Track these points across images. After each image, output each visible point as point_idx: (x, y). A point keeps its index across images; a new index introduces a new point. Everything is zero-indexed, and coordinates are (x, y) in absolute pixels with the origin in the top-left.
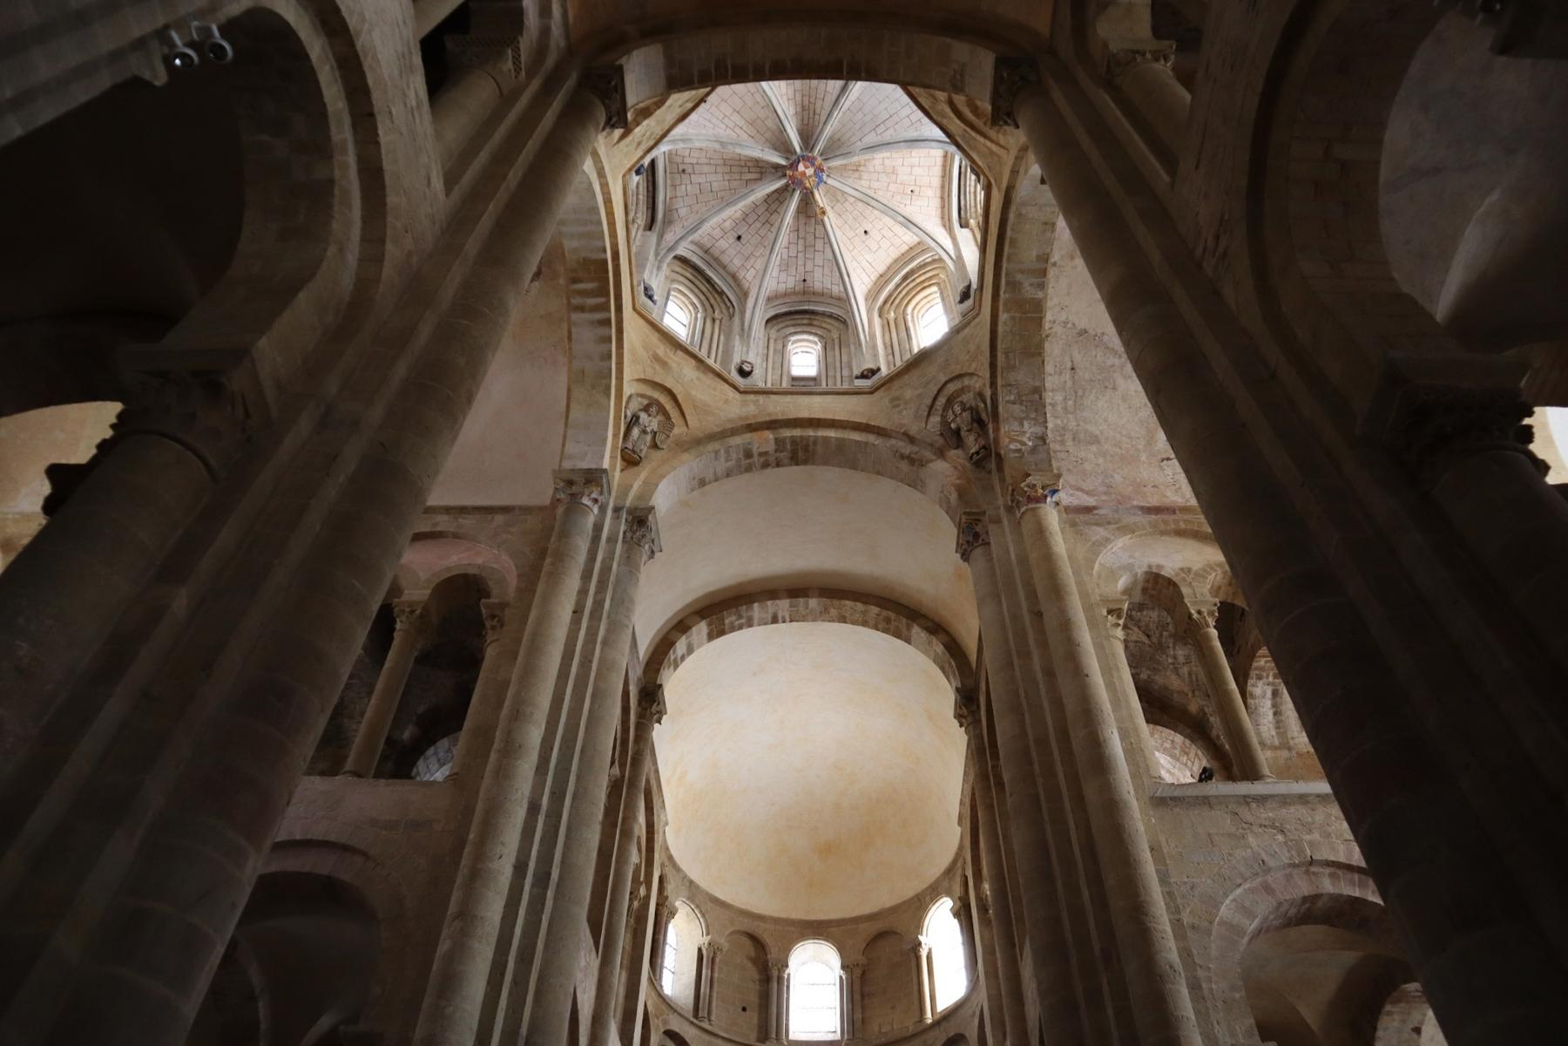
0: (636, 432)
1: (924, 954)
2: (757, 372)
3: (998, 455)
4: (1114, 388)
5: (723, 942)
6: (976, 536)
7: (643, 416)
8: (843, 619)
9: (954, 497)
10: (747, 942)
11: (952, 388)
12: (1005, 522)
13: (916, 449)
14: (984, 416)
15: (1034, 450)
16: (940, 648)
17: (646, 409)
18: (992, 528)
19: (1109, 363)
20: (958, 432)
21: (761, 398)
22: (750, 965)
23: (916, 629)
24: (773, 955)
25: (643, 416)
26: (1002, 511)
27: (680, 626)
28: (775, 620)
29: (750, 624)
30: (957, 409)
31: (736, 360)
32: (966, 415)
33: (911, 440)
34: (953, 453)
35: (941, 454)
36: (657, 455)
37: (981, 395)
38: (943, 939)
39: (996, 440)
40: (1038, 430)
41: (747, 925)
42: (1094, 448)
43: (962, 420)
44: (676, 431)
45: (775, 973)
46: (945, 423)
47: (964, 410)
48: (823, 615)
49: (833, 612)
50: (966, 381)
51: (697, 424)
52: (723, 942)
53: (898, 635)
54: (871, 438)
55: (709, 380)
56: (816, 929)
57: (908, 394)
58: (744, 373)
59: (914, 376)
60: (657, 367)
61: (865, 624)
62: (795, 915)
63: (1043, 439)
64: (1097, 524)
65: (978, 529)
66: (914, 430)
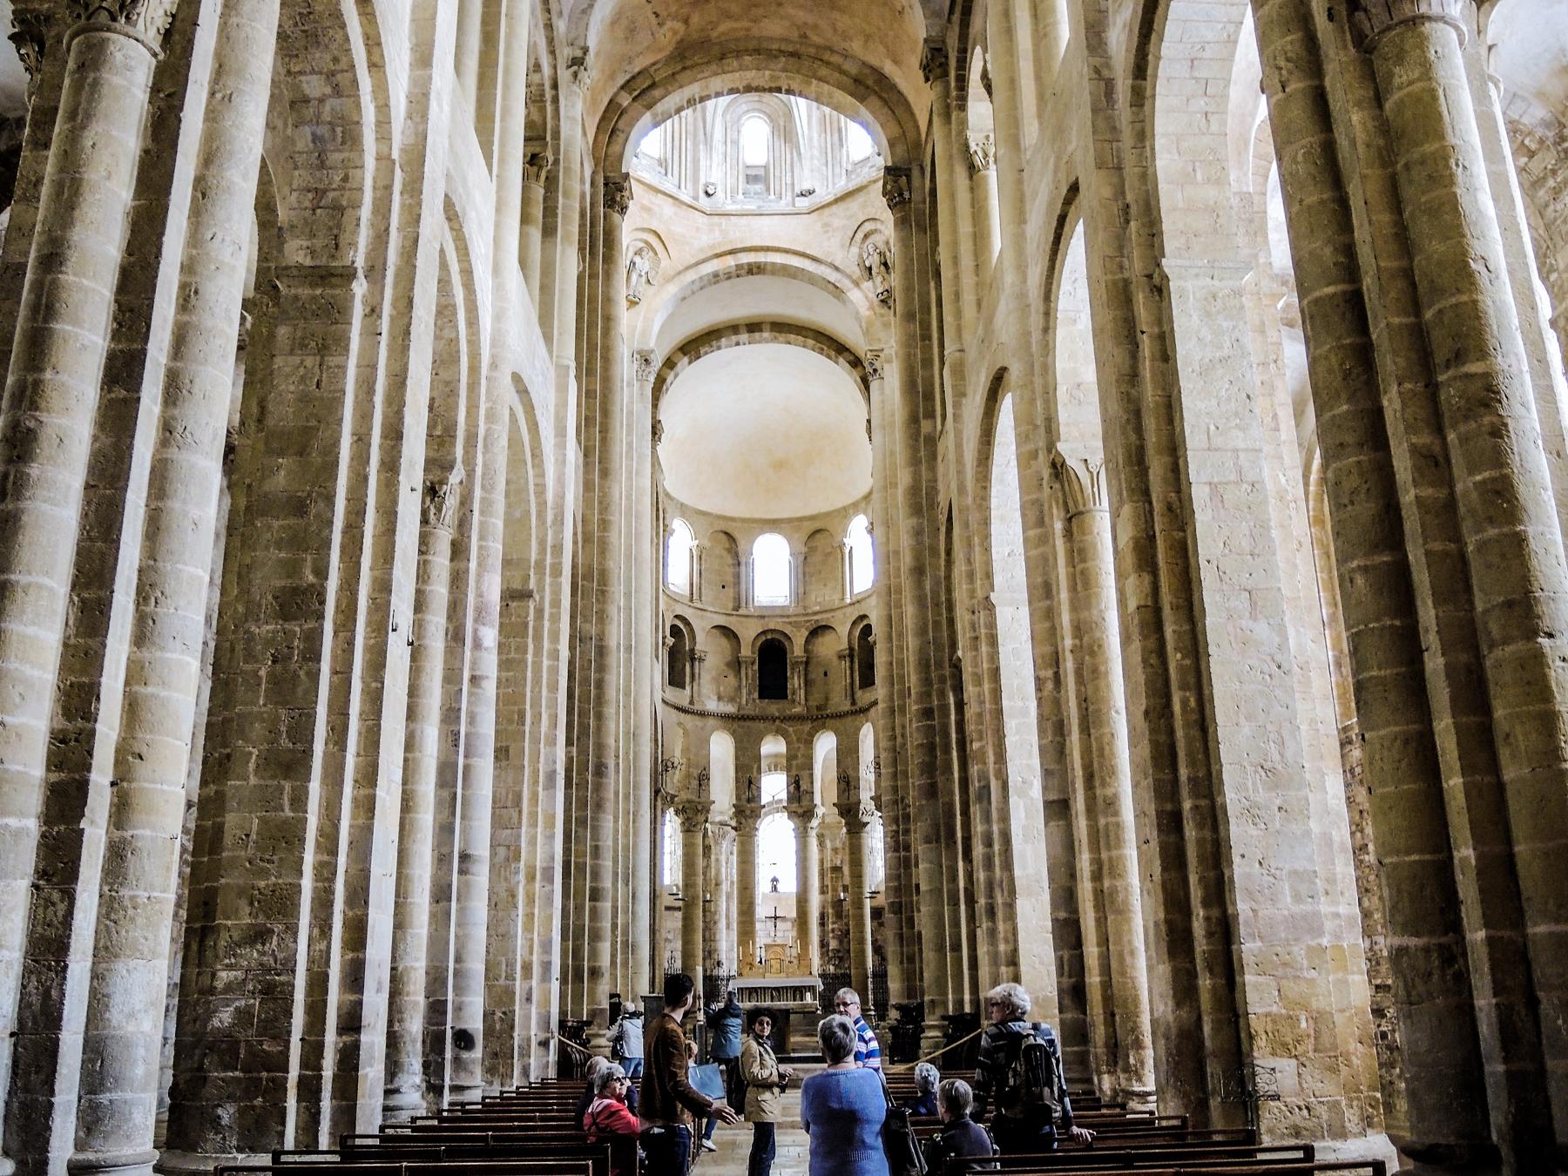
0: (634, 277)
2: (720, 195)
5: (707, 544)
6: (875, 370)
7: (637, 259)
10: (724, 537)
11: (868, 227)
17: (639, 252)
18: (886, 366)
20: (870, 269)
21: (723, 220)
22: (725, 553)
23: (841, 360)
24: (742, 545)
25: (637, 259)
27: (670, 364)
28: (738, 344)
29: (719, 348)
31: (702, 181)
32: (876, 257)
33: (837, 269)
34: (867, 285)
35: (857, 284)
36: (651, 290)
38: (859, 539)
41: (723, 526)
43: (874, 261)
44: (663, 264)
45: (743, 560)
46: (861, 256)
50: (879, 226)
51: (681, 255)
52: (707, 544)
53: (829, 357)
55: (685, 211)
56: (773, 525)
57: (836, 222)
58: (707, 193)
59: (838, 209)
60: (645, 215)
62: (757, 515)
65: (877, 365)
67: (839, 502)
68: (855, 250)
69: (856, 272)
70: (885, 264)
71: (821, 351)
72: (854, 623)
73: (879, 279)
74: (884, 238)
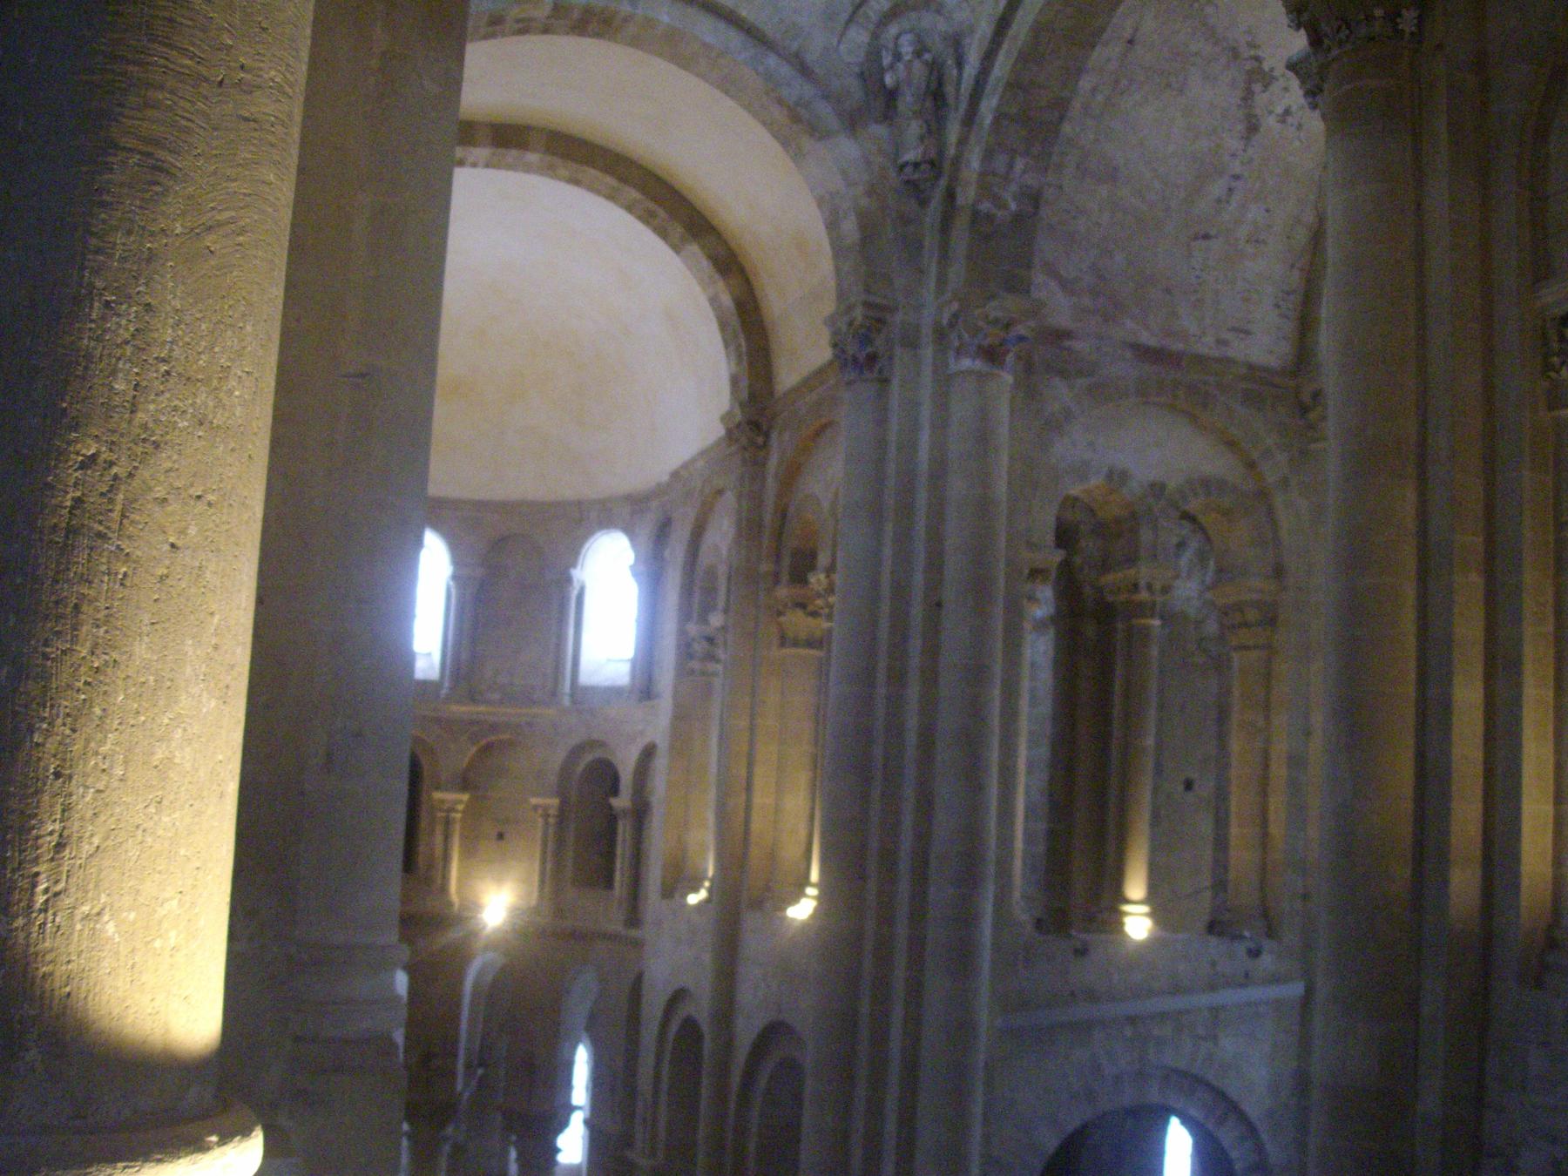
1: (574, 593)
3: (950, 196)
4: (1181, 91)
8: (575, 181)
9: (850, 226)
12: (928, 352)
13: (808, 90)
14: (949, 89)
15: (1018, 218)
16: (727, 300)
19: (1193, 48)
20: (892, 95)
23: (694, 248)
26: (927, 333)
30: (907, 50)
32: (918, 69)
33: (805, 71)
35: (853, 122)
37: (956, 43)
39: (957, 161)
40: (1031, 180)
42: (1103, 191)
43: (906, 74)
46: (874, 53)
47: (918, 54)
48: (549, 171)
49: (563, 172)
53: (662, 233)
54: (734, 38)
61: (611, 197)
63: (1034, 199)
64: (1062, 373)
66: (815, 46)
67: (567, 487)
68: (859, 37)
69: (854, 85)
70: (936, 96)
71: (647, 218)
72: (577, 752)
73: (914, 128)
74: (942, 26)
